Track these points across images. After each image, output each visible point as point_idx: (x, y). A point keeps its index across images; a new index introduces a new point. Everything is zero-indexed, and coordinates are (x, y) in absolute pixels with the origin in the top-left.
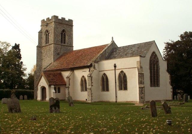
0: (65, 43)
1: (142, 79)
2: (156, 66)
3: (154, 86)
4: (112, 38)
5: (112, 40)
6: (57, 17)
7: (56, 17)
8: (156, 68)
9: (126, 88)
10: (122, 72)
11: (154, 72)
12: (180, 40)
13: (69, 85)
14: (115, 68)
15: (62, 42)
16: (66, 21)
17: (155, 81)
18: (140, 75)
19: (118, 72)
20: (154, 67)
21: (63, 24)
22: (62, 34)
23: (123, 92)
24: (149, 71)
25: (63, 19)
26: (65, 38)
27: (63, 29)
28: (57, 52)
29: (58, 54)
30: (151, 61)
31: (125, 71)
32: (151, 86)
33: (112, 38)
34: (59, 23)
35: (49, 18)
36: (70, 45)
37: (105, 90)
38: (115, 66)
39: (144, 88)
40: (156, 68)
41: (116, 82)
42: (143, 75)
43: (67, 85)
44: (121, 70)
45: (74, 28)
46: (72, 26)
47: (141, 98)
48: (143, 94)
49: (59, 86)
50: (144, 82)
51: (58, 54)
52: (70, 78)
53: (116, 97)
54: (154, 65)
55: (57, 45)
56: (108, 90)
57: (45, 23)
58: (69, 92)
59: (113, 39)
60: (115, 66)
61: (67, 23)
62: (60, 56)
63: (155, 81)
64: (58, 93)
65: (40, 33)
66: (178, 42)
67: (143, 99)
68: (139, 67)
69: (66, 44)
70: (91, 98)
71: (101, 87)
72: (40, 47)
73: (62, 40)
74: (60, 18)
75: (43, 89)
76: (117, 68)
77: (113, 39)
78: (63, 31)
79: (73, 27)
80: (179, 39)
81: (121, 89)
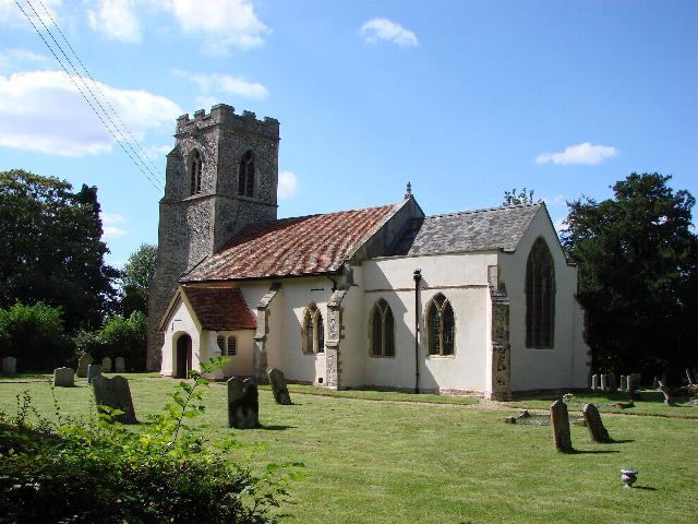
0: (250, 194)
2: (544, 283)
3: (538, 345)
6: (231, 109)
7: (226, 110)
8: (544, 289)
9: (449, 349)
10: (440, 298)
12: (614, 199)
15: (241, 192)
17: (540, 329)
19: (427, 297)
20: (539, 286)
22: (243, 164)
24: (524, 296)
25: (249, 116)
30: (529, 264)
31: (444, 292)
32: (529, 345)
38: (418, 278)
39: (507, 352)
40: (544, 289)
42: (508, 312)
44: (436, 292)
46: (276, 140)
48: (504, 369)
50: (508, 333)
53: (418, 375)
54: (539, 279)
56: (390, 352)
57: (191, 129)
59: (409, 190)
63: (540, 329)
66: (607, 204)
68: (495, 284)
69: (254, 200)
70: (339, 376)
71: (368, 344)
74: (239, 112)
75: (183, 342)
77: (409, 190)
78: (249, 155)
80: (612, 196)
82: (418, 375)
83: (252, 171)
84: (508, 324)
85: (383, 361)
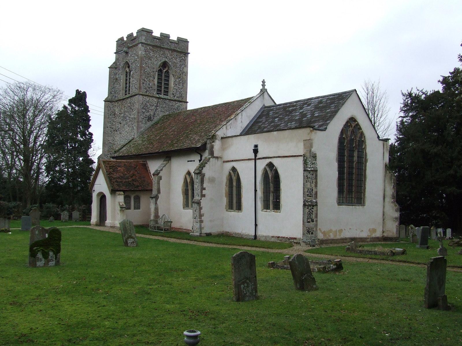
0: (166, 93)
1: (313, 185)
2: (356, 154)
3: (350, 203)
4: (264, 82)
5: (261, 87)
6: (149, 32)
7: (145, 32)
8: (355, 159)
9: (277, 206)
10: (271, 165)
11: (351, 167)
12: (441, 92)
13: (159, 191)
14: (256, 156)
15: (159, 91)
16: (173, 42)
17: (351, 188)
18: (309, 176)
19: (262, 165)
20: (351, 156)
21: (163, 48)
22: (160, 71)
23: (271, 214)
24: (336, 165)
25: (165, 37)
26: (168, 81)
27: (164, 60)
28: (148, 114)
29: (150, 119)
31: (275, 162)
32: (340, 203)
33: (264, 82)
34: (153, 46)
35: (132, 34)
36: (180, 99)
37: (271, 206)
38: (256, 151)
39: (315, 208)
40: (355, 159)
41: (256, 191)
42: (316, 176)
43: (154, 193)
44: (268, 161)
45: (191, 58)
46: (186, 54)
47: (308, 232)
48: (313, 221)
49: (137, 193)
50: (316, 193)
51: (150, 119)
52: (160, 175)
53: (256, 225)
54: (351, 151)
55: (148, 99)
56: (239, 208)
57: (125, 46)
58: (156, 209)
59: (263, 85)
60: (256, 151)
61: (173, 47)
62: (153, 122)
63: (351, 188)
64: (135, 208)
65: (113, 68)
66: (436, 94)
67: (312, 233)
68: (308, 155)
69: (170, 96)
70: (201, 225)
71: (225, 201)
72: (111, 102)
73: (159, 87)
74: (156, 34)
75: (102, 198)
76: (259, 156)
77: (263, 85)
78: (165, 65)
79: (187, 57)
80: (440, 88)
81: (266, 207)
82: (256, 225)
83: (167, 76)
84: (316, 186)
85: (233, 214)
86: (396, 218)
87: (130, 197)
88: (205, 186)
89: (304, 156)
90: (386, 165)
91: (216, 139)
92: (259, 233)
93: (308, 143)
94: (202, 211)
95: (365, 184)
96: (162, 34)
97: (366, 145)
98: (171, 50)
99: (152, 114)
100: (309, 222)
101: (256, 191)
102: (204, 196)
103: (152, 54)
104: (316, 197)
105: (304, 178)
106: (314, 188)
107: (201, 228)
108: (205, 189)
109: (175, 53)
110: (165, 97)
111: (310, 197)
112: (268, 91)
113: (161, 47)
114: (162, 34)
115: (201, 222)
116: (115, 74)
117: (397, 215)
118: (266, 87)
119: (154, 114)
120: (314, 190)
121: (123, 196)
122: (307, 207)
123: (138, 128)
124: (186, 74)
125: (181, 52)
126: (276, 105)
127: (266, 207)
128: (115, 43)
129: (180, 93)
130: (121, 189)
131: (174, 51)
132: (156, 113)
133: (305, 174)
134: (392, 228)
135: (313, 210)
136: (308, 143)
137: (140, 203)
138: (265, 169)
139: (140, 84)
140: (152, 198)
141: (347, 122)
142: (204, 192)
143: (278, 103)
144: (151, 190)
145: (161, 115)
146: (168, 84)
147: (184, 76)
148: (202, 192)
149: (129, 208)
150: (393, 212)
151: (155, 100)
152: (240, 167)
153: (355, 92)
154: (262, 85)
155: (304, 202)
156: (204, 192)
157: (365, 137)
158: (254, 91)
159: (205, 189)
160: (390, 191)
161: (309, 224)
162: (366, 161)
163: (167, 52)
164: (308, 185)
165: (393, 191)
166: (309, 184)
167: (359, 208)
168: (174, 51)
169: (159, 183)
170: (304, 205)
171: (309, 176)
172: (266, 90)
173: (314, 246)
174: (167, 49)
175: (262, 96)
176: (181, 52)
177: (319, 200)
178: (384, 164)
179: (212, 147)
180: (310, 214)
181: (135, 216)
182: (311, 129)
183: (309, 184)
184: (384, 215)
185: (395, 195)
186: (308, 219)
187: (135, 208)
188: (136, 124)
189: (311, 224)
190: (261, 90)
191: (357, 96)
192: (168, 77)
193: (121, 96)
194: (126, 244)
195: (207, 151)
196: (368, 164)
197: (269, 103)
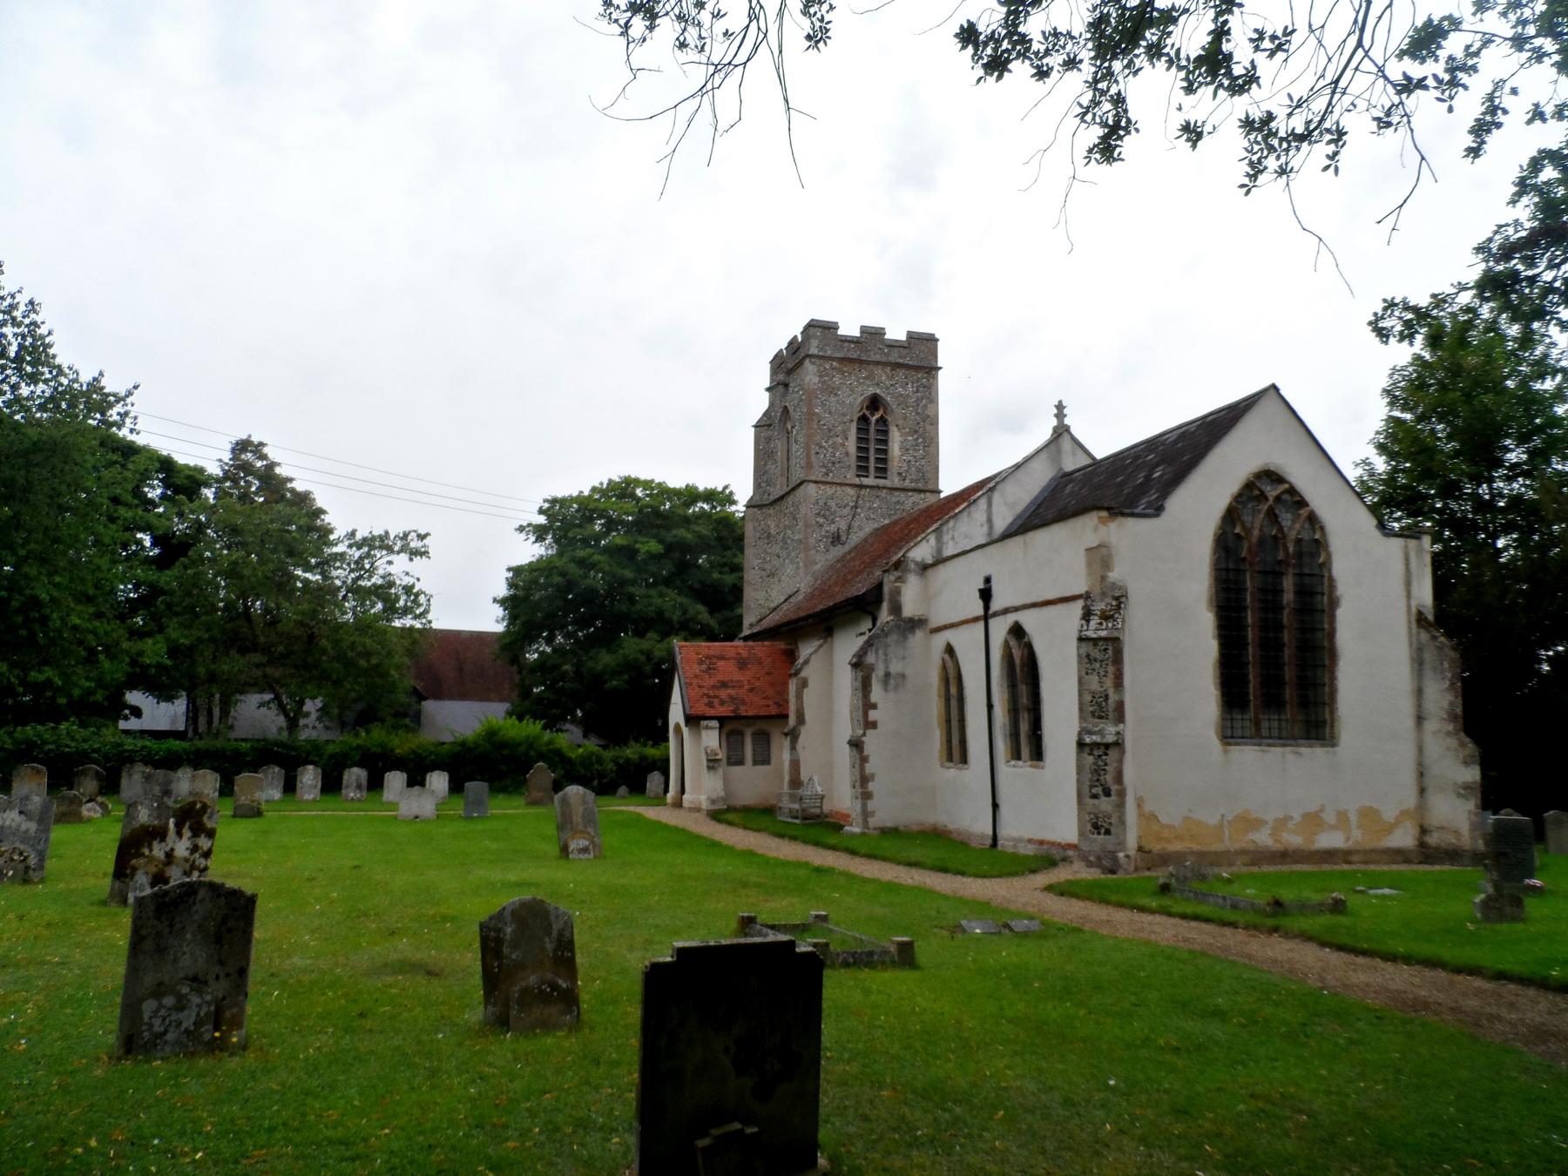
0: (882, 472)
1: (1109, 682)
2: (1288, 584)
4: (1060, 407)
5: (1054, 422)
6: (829, 328)
7: (820, 329)
10: (1017, 631)
11: (1271, 627)
13: (801, 719)
14: (987, 607)
15: (863, 469)
16: (894, 345)
18: (1096, 653)
19: (999, 628)
21: (868, 363)
22: (863, 419)
23: (1024, 768)
25: (872, 335)
26: (885, 442)
27: (871, 390)
28: (833, 528)
29: (836, 539)
31: (1028, 620)
32: (1229, 736)
33: (1060, 407)
34: (842, 360)
36: (920, 486)
38: (986, 595)
41: (990, 706)
43: (792, 721)
44: (1011, 619)
45: (946, 383)
46: (932, 370)
47: (1096, 827)
48: (1107, 793)
49: (760, 725)
50: (1120, 706)
51: (836, 539)
52: (803, 674)
53: (995, 806)
55: (830, 490)
56: (964, 759)
58: (795, 765)
60: (986, 595)
61: (894, 357)
62: (847, 548)
64: (755, 763)
65: (763, 426)
67: (1108, 832)
69: (895, 481)
70: (864, 807)
72: (760, 507)
73: (863, 458)
74: (849, 329)
76: (996, 605)
78: (875, 403)
79: (935, 378)
81: (1016, 755)
82: (995, 806)
83: (884, 432)
84: (1119, 683)
85: (953, 773)
86: (1467, 787)
87: (741, 734)
88: (874, 698)
89: (1086, 596)
90: (1421, 619)
91: (907, 570)
92: (1008, 831)
93: (1100, 557)
94: (869, 768)
95: (1333, 678)
96: (864, 330)
97: (1329, 556)
98: (885, 364)
99: (843, 527)
100: (1095, 796)
101: (990, 706)
102: (874, 725)
103: (837, 380)
104: (1120, 718)
105: (1080, 662)
106: (1111, 692)
107: (866, 814)
108: (874, 706)
109: (901, 373)
110: (881, 482)
111: (1101, 717)
112: (1073, 431)
113: (860, 362)
114: (864, 330)
115: (866, 796)
116: (768, 440)
117: (1473, 774)
118: (1067, 421)
119: (849, 527)
120: (1113, 697)
121: (716, 733)
122: (1087, 750)
123: (809, 563)
124: (934, 422)
125: (917, 368)
126: (1096, 463)
127: (1016, 755)
128: (768, 367)
129: (919, 470)
130: (712, 712)
131: (896, 366)
132: (856, 524)
133: (1083, 651)
134: (1457, 816)
135: (1108, 759)
136: (1100, 557)
137: (769, 749)
138: (1006, 642)
139: (808, 456)
140: (786, 735)
141: (1249, 486)
142: (873, 715)
143: (1099, 455)
144: (786, 717)
145: (869, 528)
146: (885, 451)
147: (928, 427)
148: (866, 715)
149: (741, 762)
150: (1457, 768)
151: (851, 491)
152: (956, 638)
153: (1272, 392)
154: (1056, 416)
155: (1080, 734)
156: (873, 715)
157: (1322, 528)
158: (767, 394)
159: (874, 706)
160: (1441, 697)
161: (1096, 801)
162: (1334, 603)
163: (878, 371)
164: (1093, 682)
165: (1449, 697)
166: (1094, 678)
167: (1314, 754)
168: (896, 366)
169: (799, 697)
170: (1081, 745)
171: (1096, 653)
172: (1067, 429)
173: (1113, 872)
174: (878, 363)
175: (1052, 447)
176: (917, 368)
177: (1130, 731)
178: (1414, 610)
179: (897, 593)
180: (1098, 771)
181: (752, 783)
182: (1104, 514)
183: (1094, 678)
184: (1421, 775)
185: (1459, 710)
186: (1091, 787)
187: (755, 763)
188: (802, 556)
189: (1105, 804)
190: (1055, 429)
191: (1283, 406)
192: (886, 432)
193: (777, 491)
194: (565, 850)
195: (885, 606)
196: (1342, 615)
197: (1071, 463)
